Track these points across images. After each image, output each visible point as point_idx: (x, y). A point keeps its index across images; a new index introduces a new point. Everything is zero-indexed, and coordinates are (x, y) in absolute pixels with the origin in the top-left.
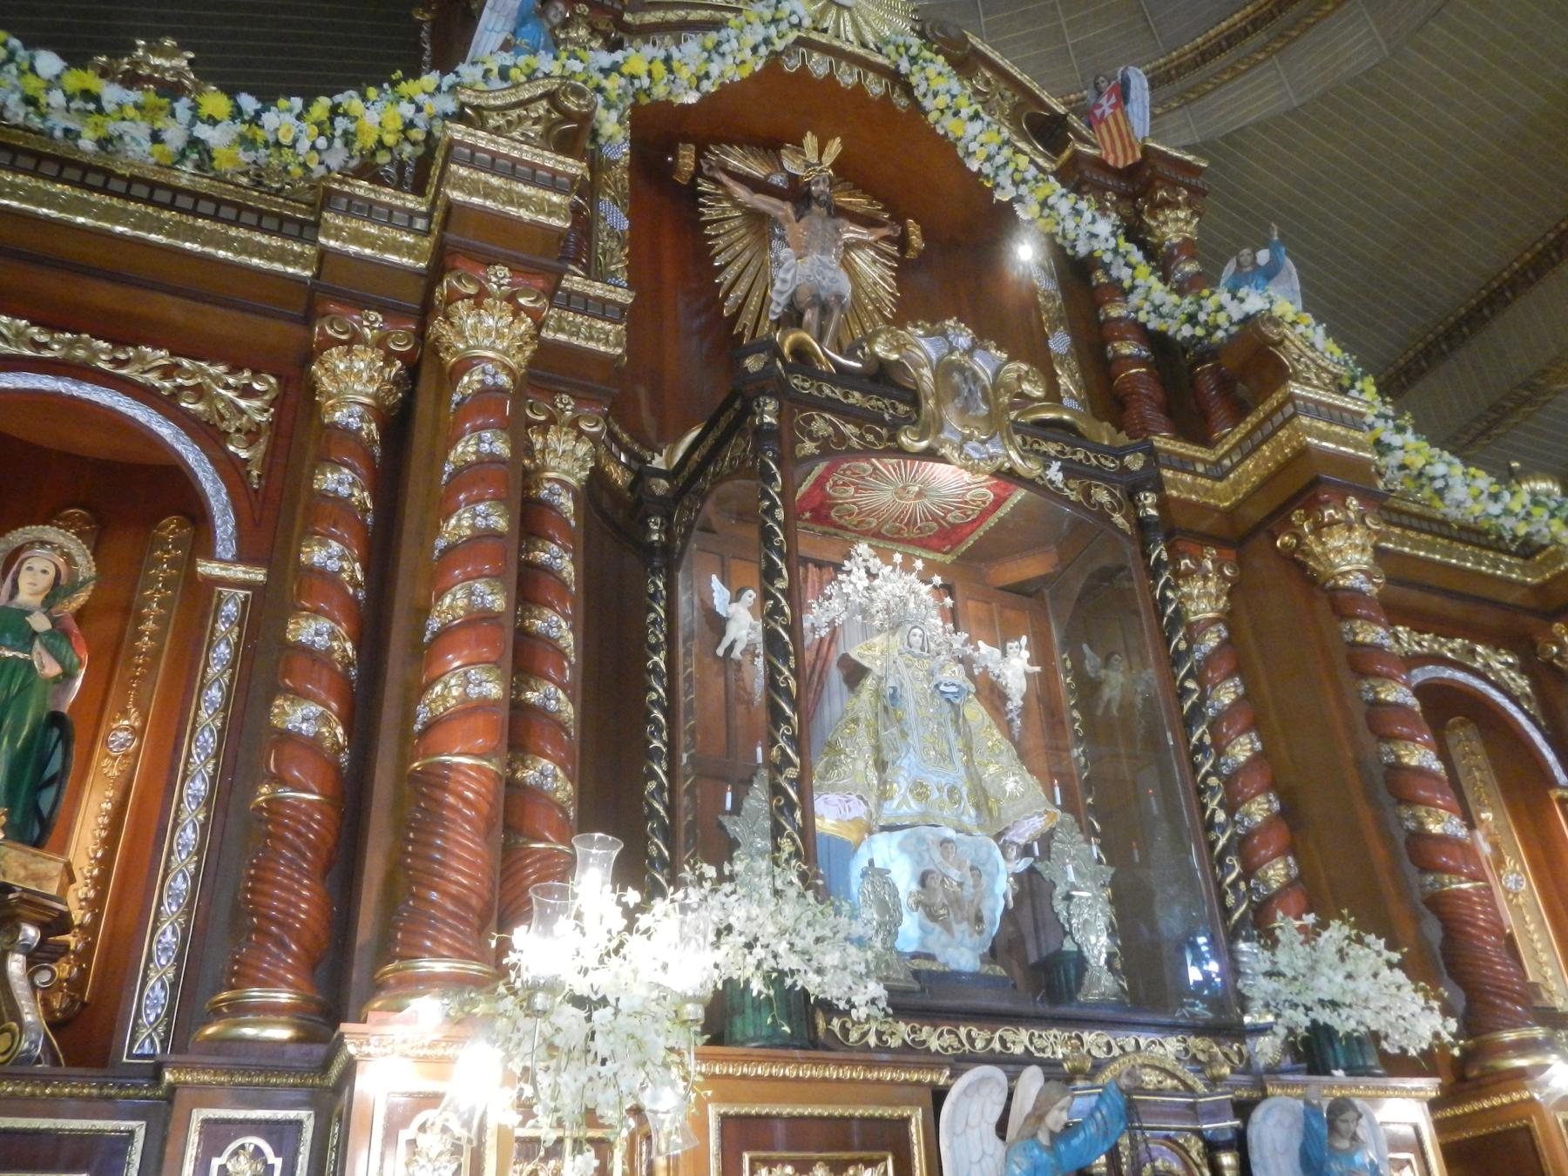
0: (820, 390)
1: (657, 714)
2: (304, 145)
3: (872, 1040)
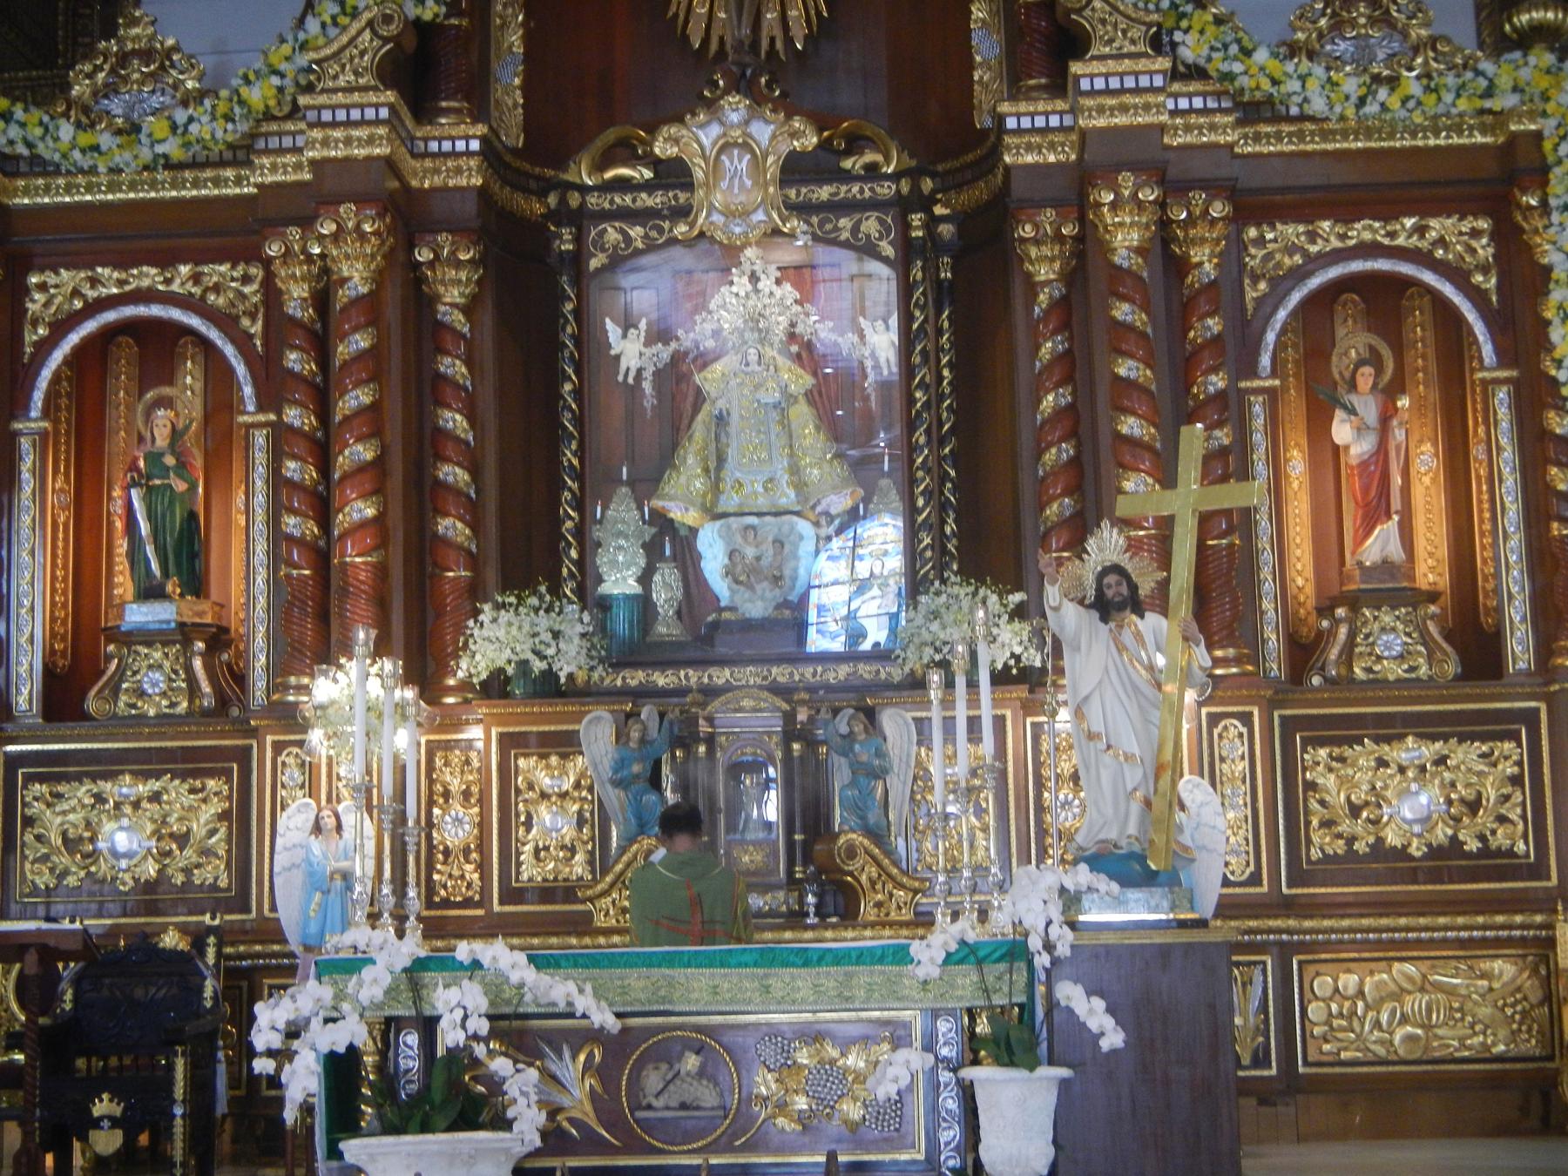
0: (612, 202)
2: (219, 134)
3: (619, 682)
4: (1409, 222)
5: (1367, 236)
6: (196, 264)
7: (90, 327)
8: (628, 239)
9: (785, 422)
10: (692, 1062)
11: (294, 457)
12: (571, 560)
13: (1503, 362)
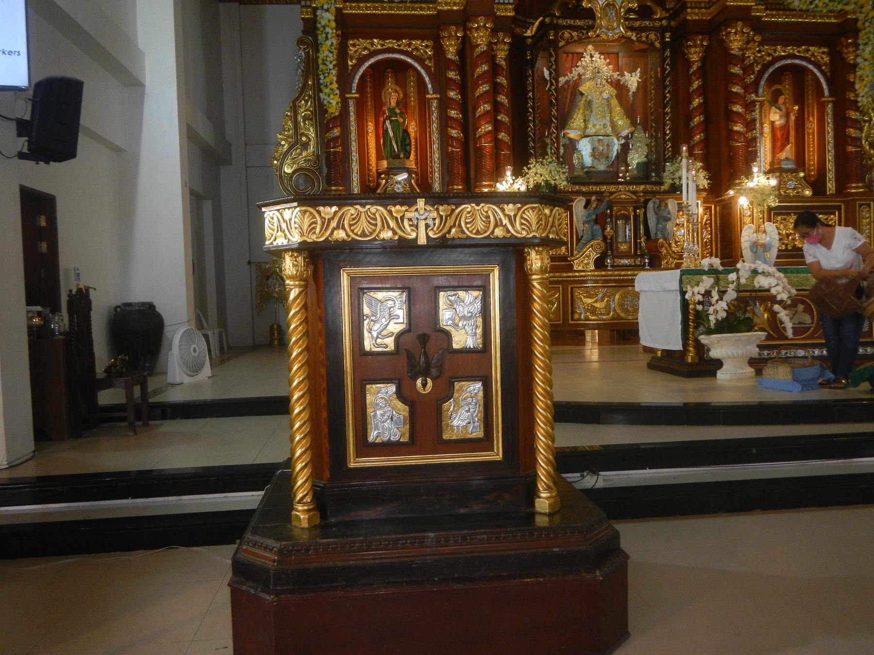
0: (567, 22)
1: (530, 110)
3: (570, 190)
4: (803, 47)
5: (791, 51)
6: (409, 40)
7: (372, 61)
8: (572, 36)
9: (609, 105)
10: (801, 307)
11: (453, 109)
12: (555, 148)
13: (831, 95)
